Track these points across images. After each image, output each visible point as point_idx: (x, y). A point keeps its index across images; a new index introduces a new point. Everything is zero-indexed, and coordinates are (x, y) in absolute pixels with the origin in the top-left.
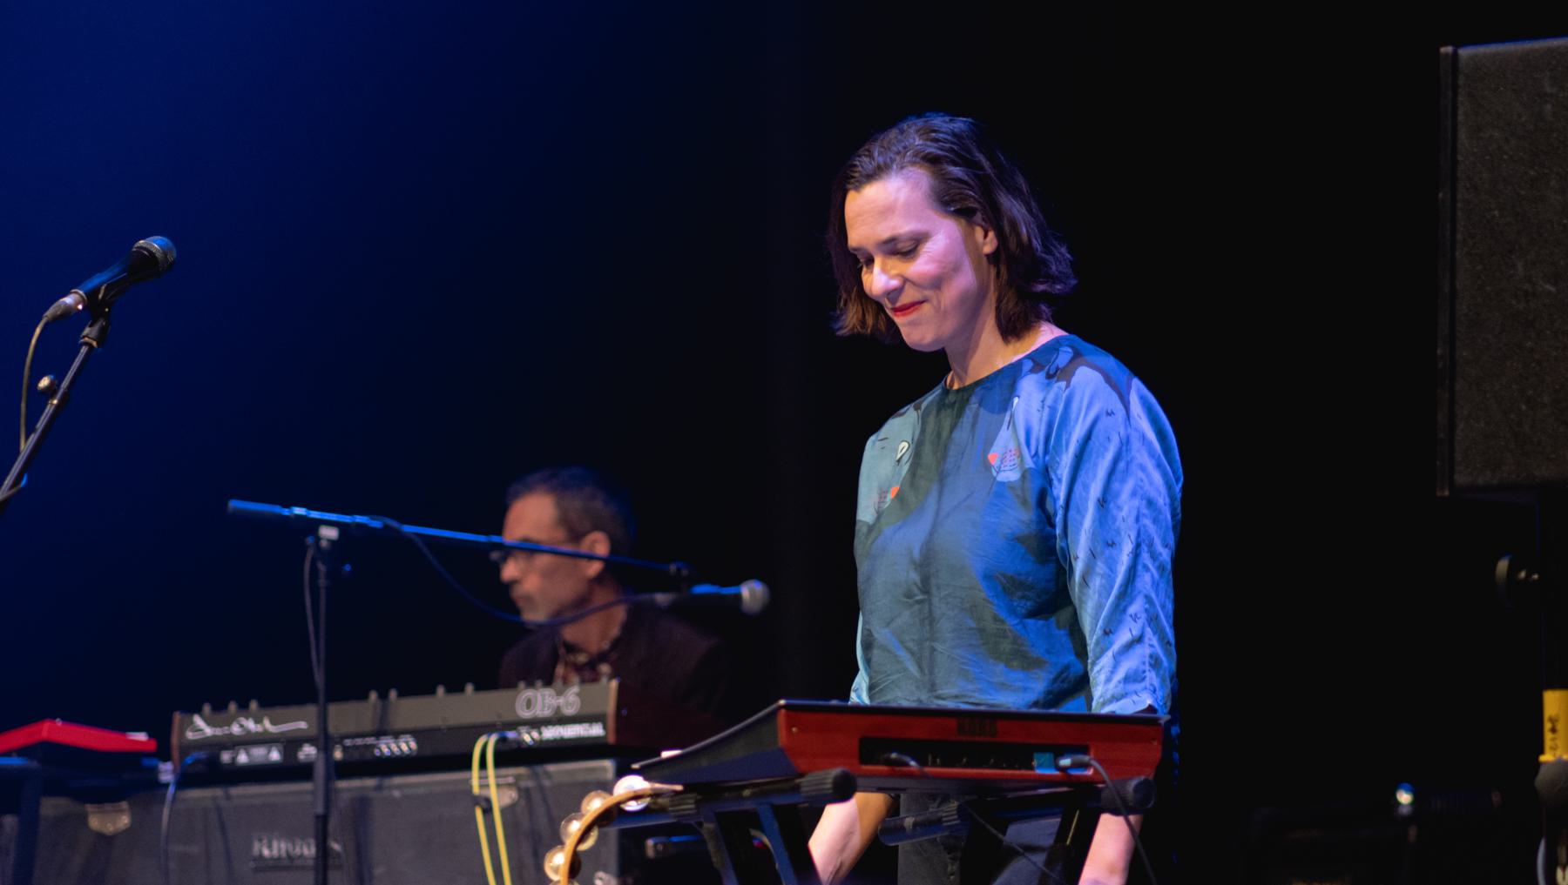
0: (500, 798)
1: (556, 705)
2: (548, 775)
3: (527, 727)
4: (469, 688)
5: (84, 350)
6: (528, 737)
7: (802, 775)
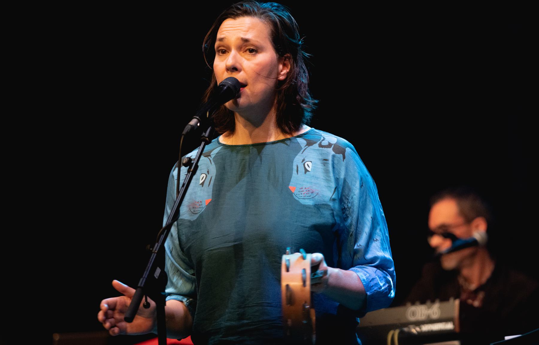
6: (414, 330)
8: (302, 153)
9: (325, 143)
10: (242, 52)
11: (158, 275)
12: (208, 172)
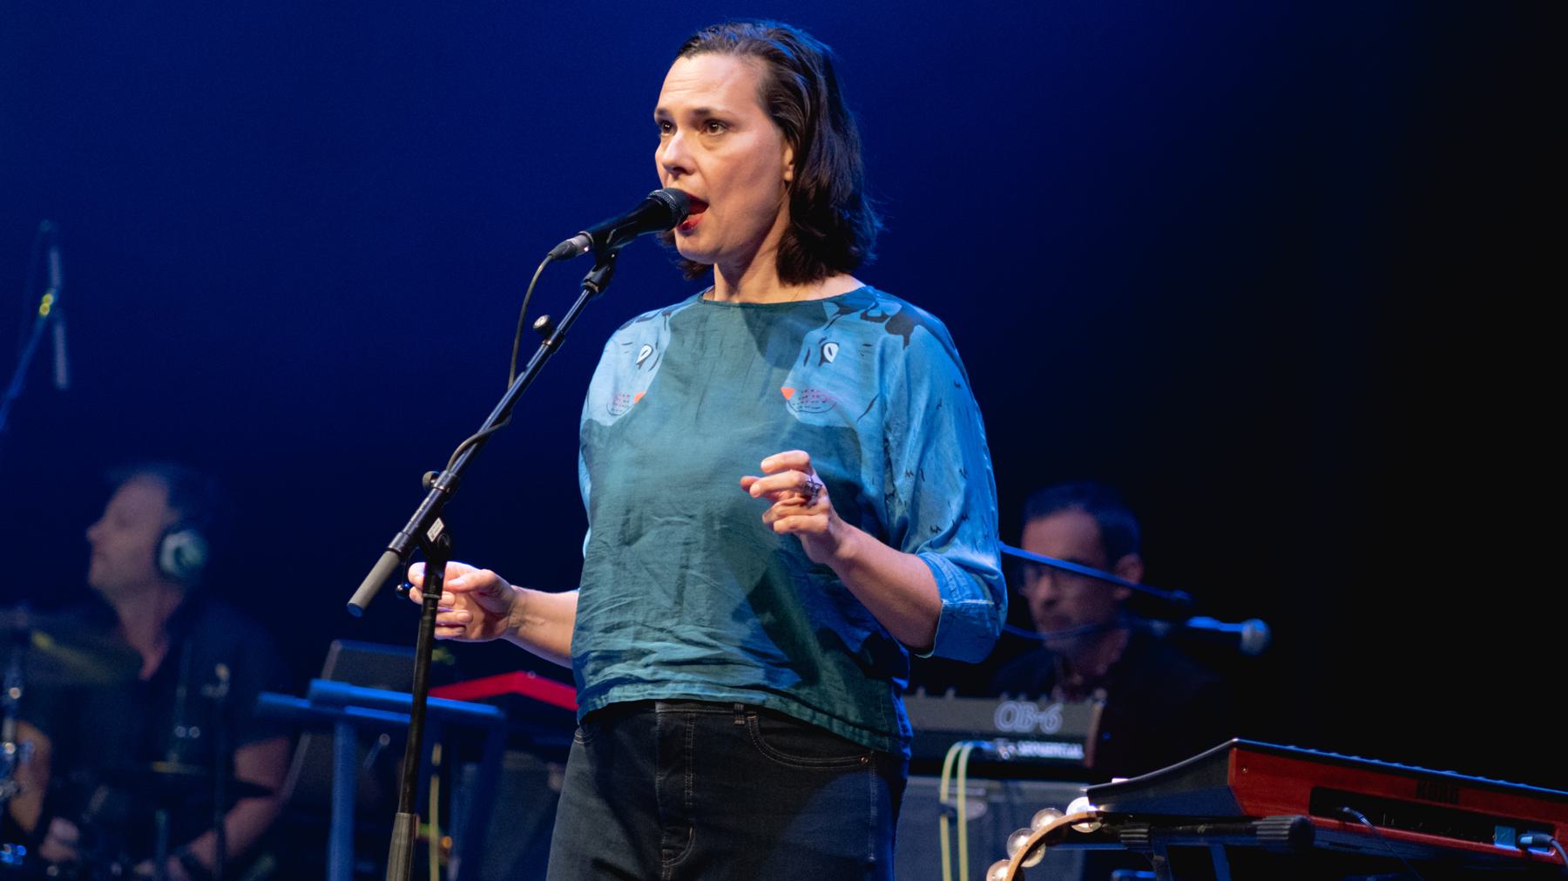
0: (965, 811)
1: (1036, 721)
2: (1020, 792)
3: (1003, 739)
4: (950, 693)
5: (585, 293)
6: (1005, 751)
7: (1259, 818)
11: (436, 535)
12: (657, 344)
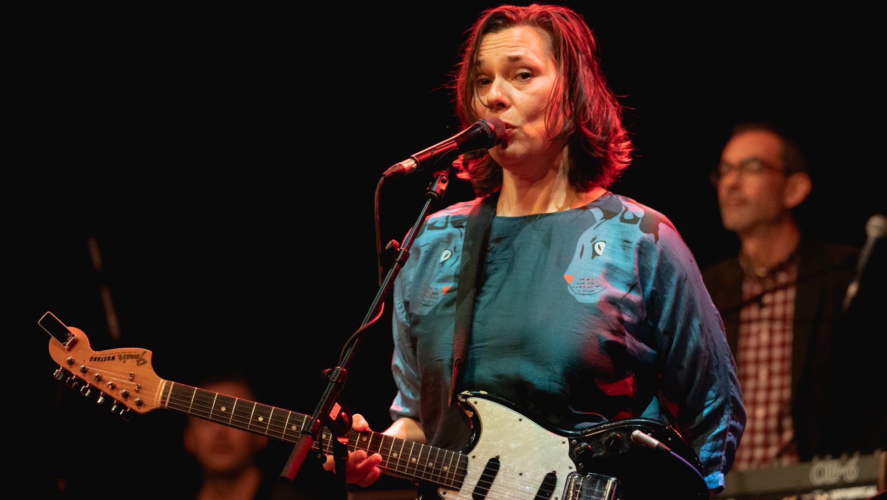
8: (594, 229)
9: (628, 216)
10: (510, 79)
